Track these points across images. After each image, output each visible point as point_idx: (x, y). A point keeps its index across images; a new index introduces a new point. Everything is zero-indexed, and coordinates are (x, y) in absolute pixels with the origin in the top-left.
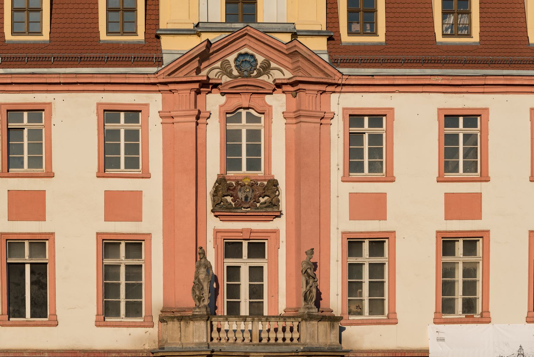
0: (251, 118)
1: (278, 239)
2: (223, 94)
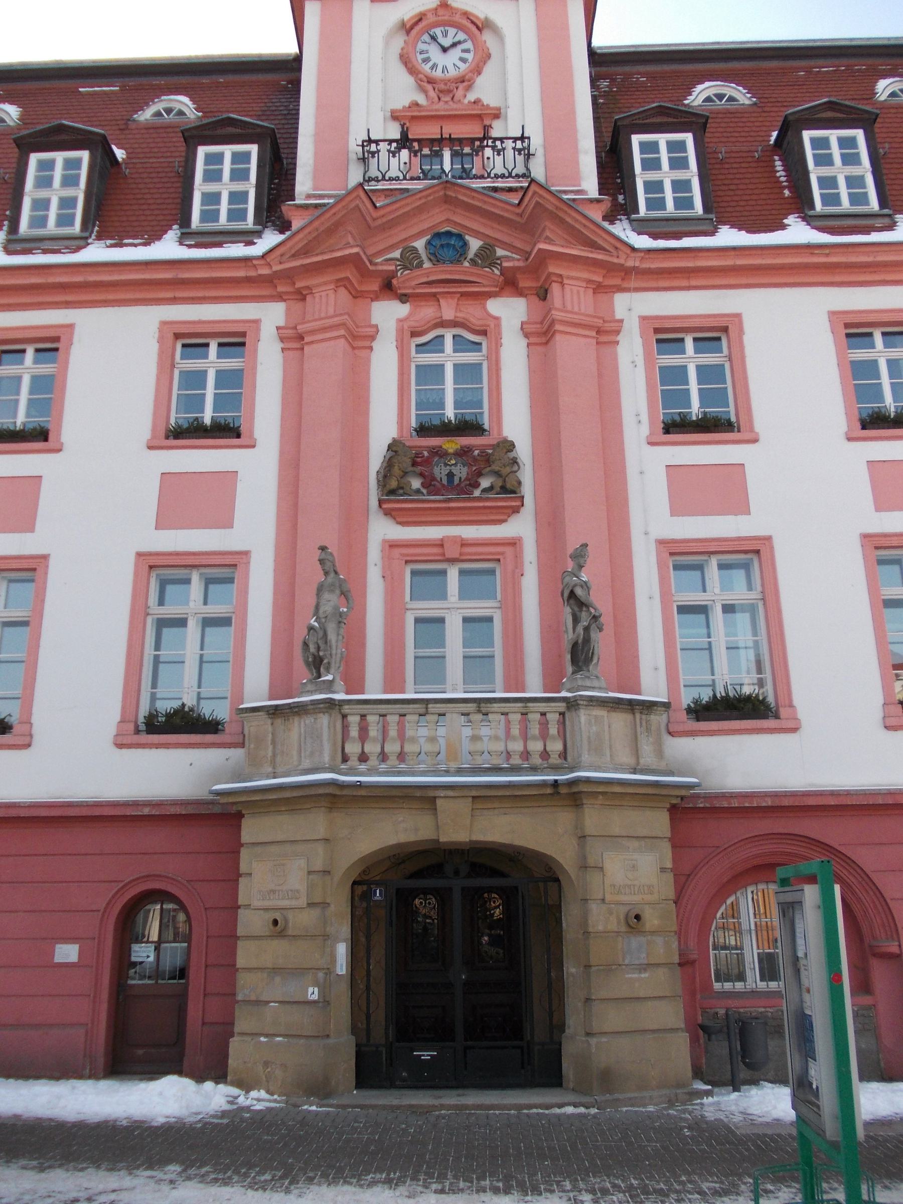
0: (460, 344)
1: (518, 558)
2: (404, 298)
